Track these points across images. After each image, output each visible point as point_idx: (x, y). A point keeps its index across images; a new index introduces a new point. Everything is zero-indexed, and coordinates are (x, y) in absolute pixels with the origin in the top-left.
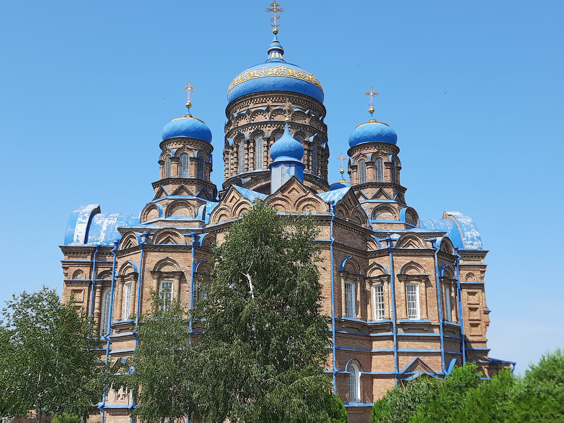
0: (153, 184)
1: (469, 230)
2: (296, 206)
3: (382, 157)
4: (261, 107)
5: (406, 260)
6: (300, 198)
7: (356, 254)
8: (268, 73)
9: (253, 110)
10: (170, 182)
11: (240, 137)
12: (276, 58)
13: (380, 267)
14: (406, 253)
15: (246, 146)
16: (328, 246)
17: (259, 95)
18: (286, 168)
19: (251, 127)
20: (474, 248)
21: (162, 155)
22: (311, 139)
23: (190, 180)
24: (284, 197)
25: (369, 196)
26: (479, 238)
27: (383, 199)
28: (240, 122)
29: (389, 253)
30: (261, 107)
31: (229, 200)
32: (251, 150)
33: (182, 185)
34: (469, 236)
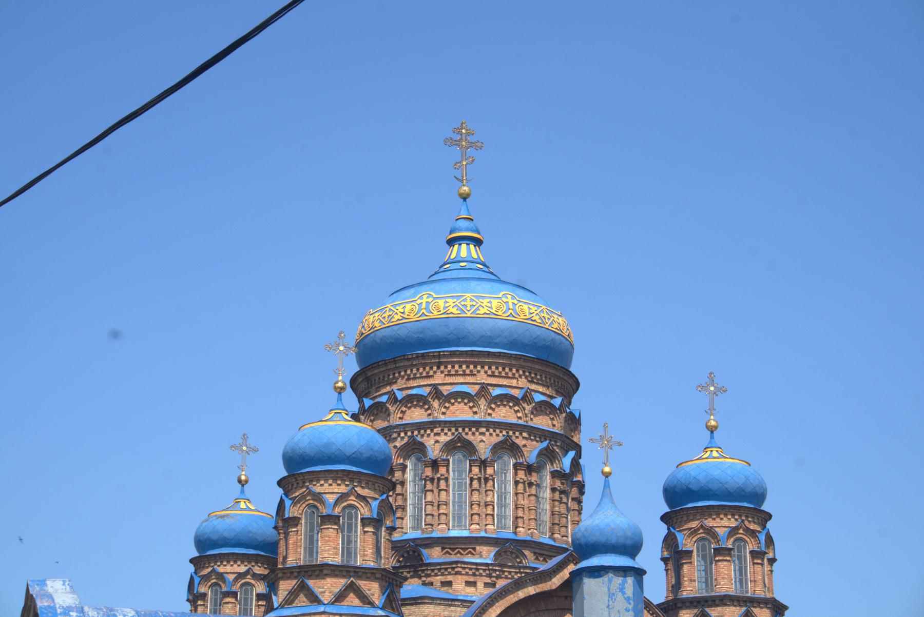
3: (746, 538)
4: (462, 384)
8: (480, 308)
9: (445, 390)
10: (325, 572)
11: (415, 449)
12: (471, 259)
15: (429, 472)
17: (459, 357)
18: (618, 580)
19: (440, 429)
23: (367, 571)
28: (407, 412)
30: (462, 384)
32: (443, 483)
33: (352, 581)
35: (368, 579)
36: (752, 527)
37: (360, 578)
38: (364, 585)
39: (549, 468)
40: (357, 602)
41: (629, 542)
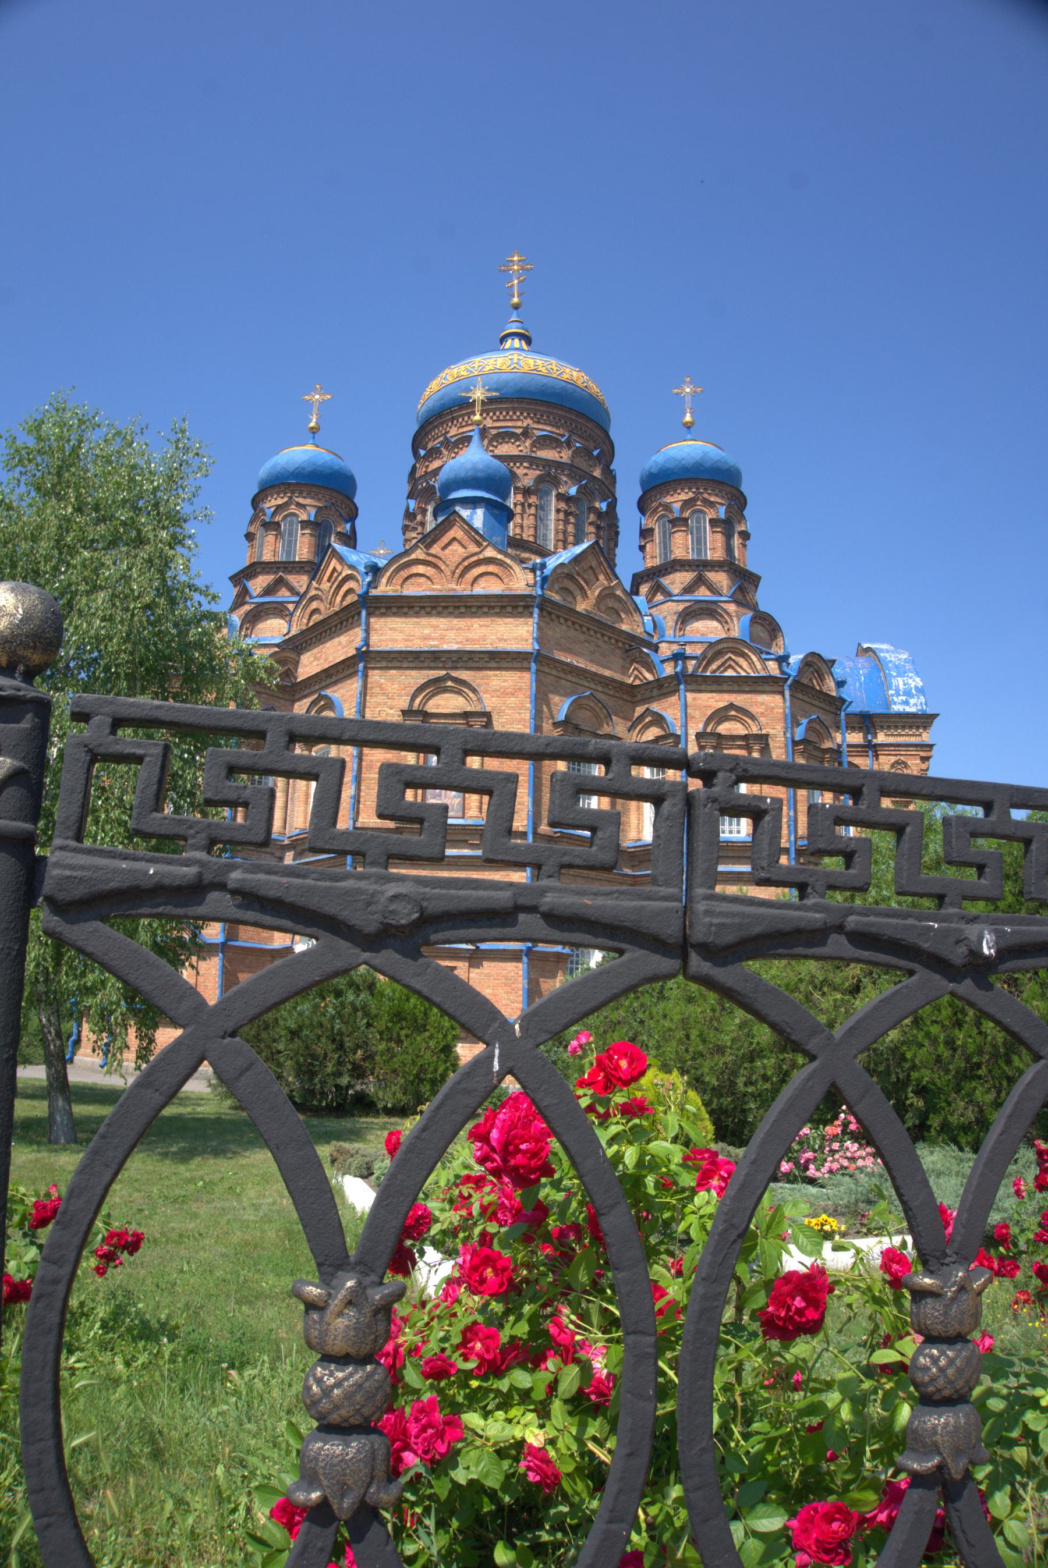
0: (231, 578)
1: (902, 673)
2: (457, 575)
5: (715, 701)
6: (467, 558)
7: (606, 690)
13: (659, 720)
14: (718, 684)
16: (525, 664)
20: (911, 709)
21: (251, 522)
22: (573, 491)
24: (430, 559)
25: (676, 589)
26: (921, 691)
27: (703, 594)
29: (679, 684)
31: (326, 578)
34: (901, 687)
35: (298, 573)
36: (712, 499)
37: (290, 572)
38: (293, 579)
39: (554, 493)
40: (288, 594)
41: (480, 474)
